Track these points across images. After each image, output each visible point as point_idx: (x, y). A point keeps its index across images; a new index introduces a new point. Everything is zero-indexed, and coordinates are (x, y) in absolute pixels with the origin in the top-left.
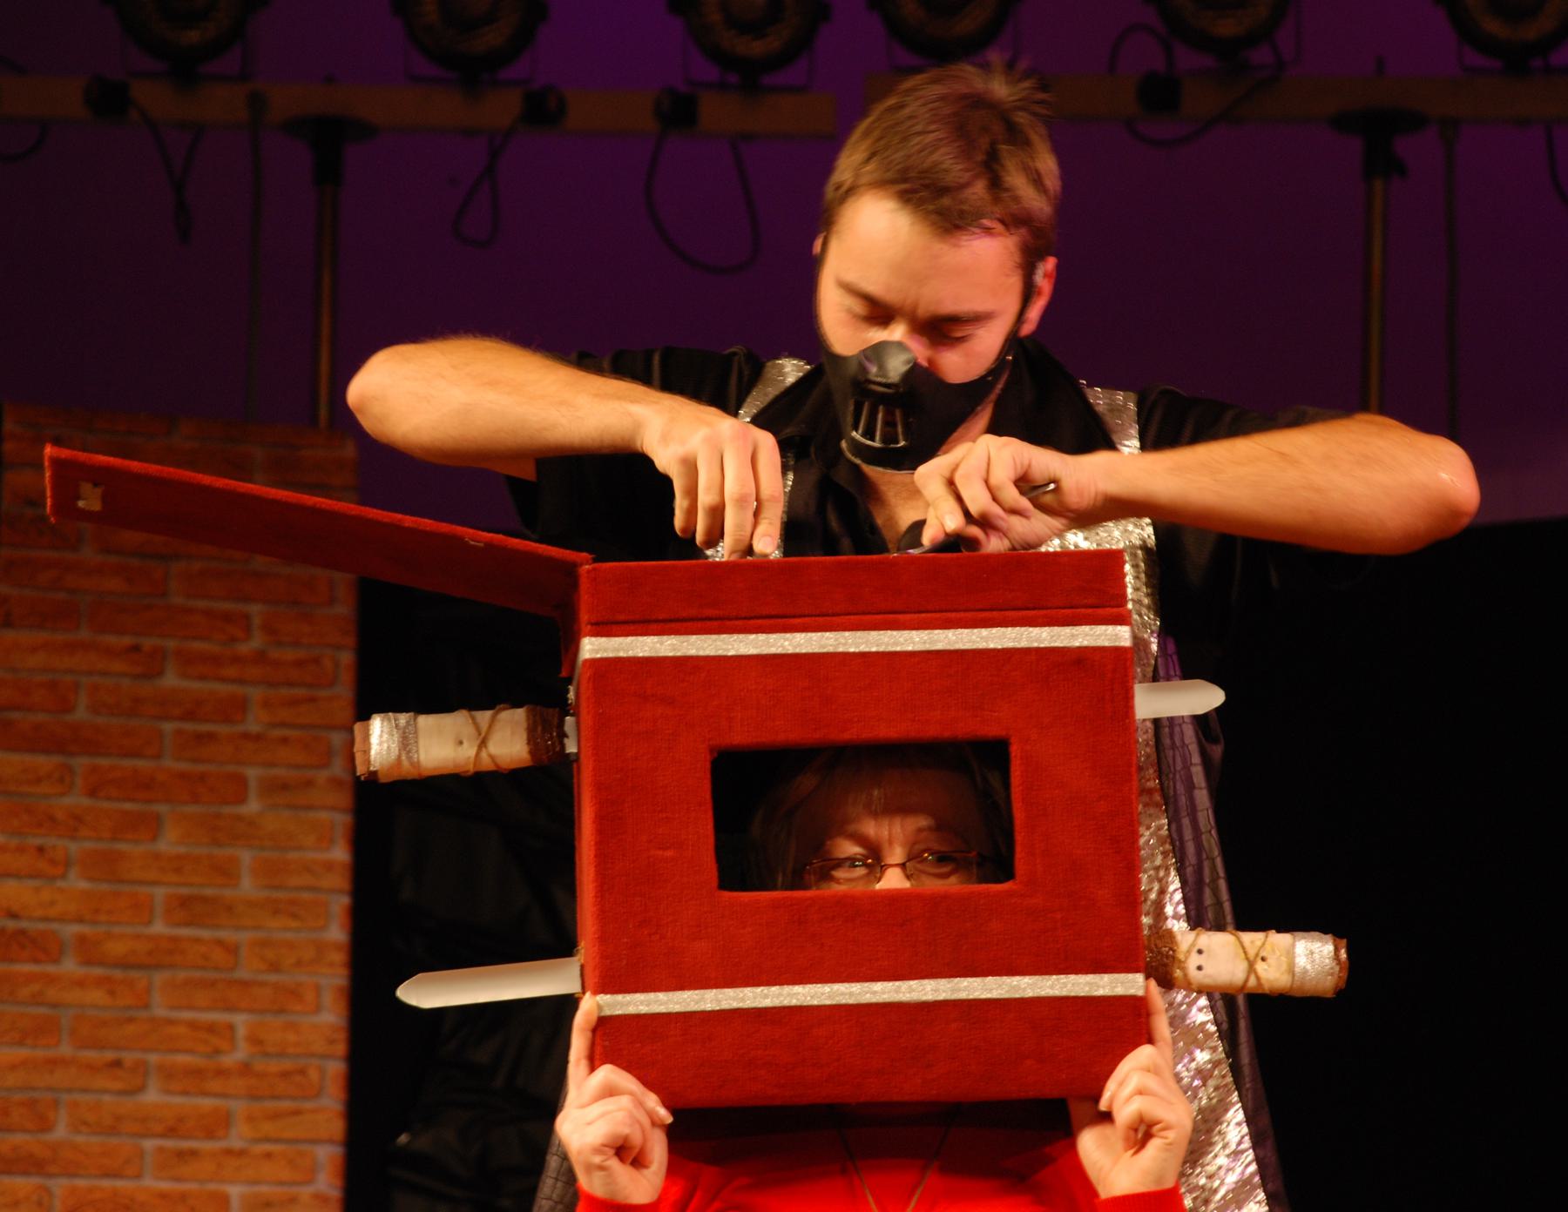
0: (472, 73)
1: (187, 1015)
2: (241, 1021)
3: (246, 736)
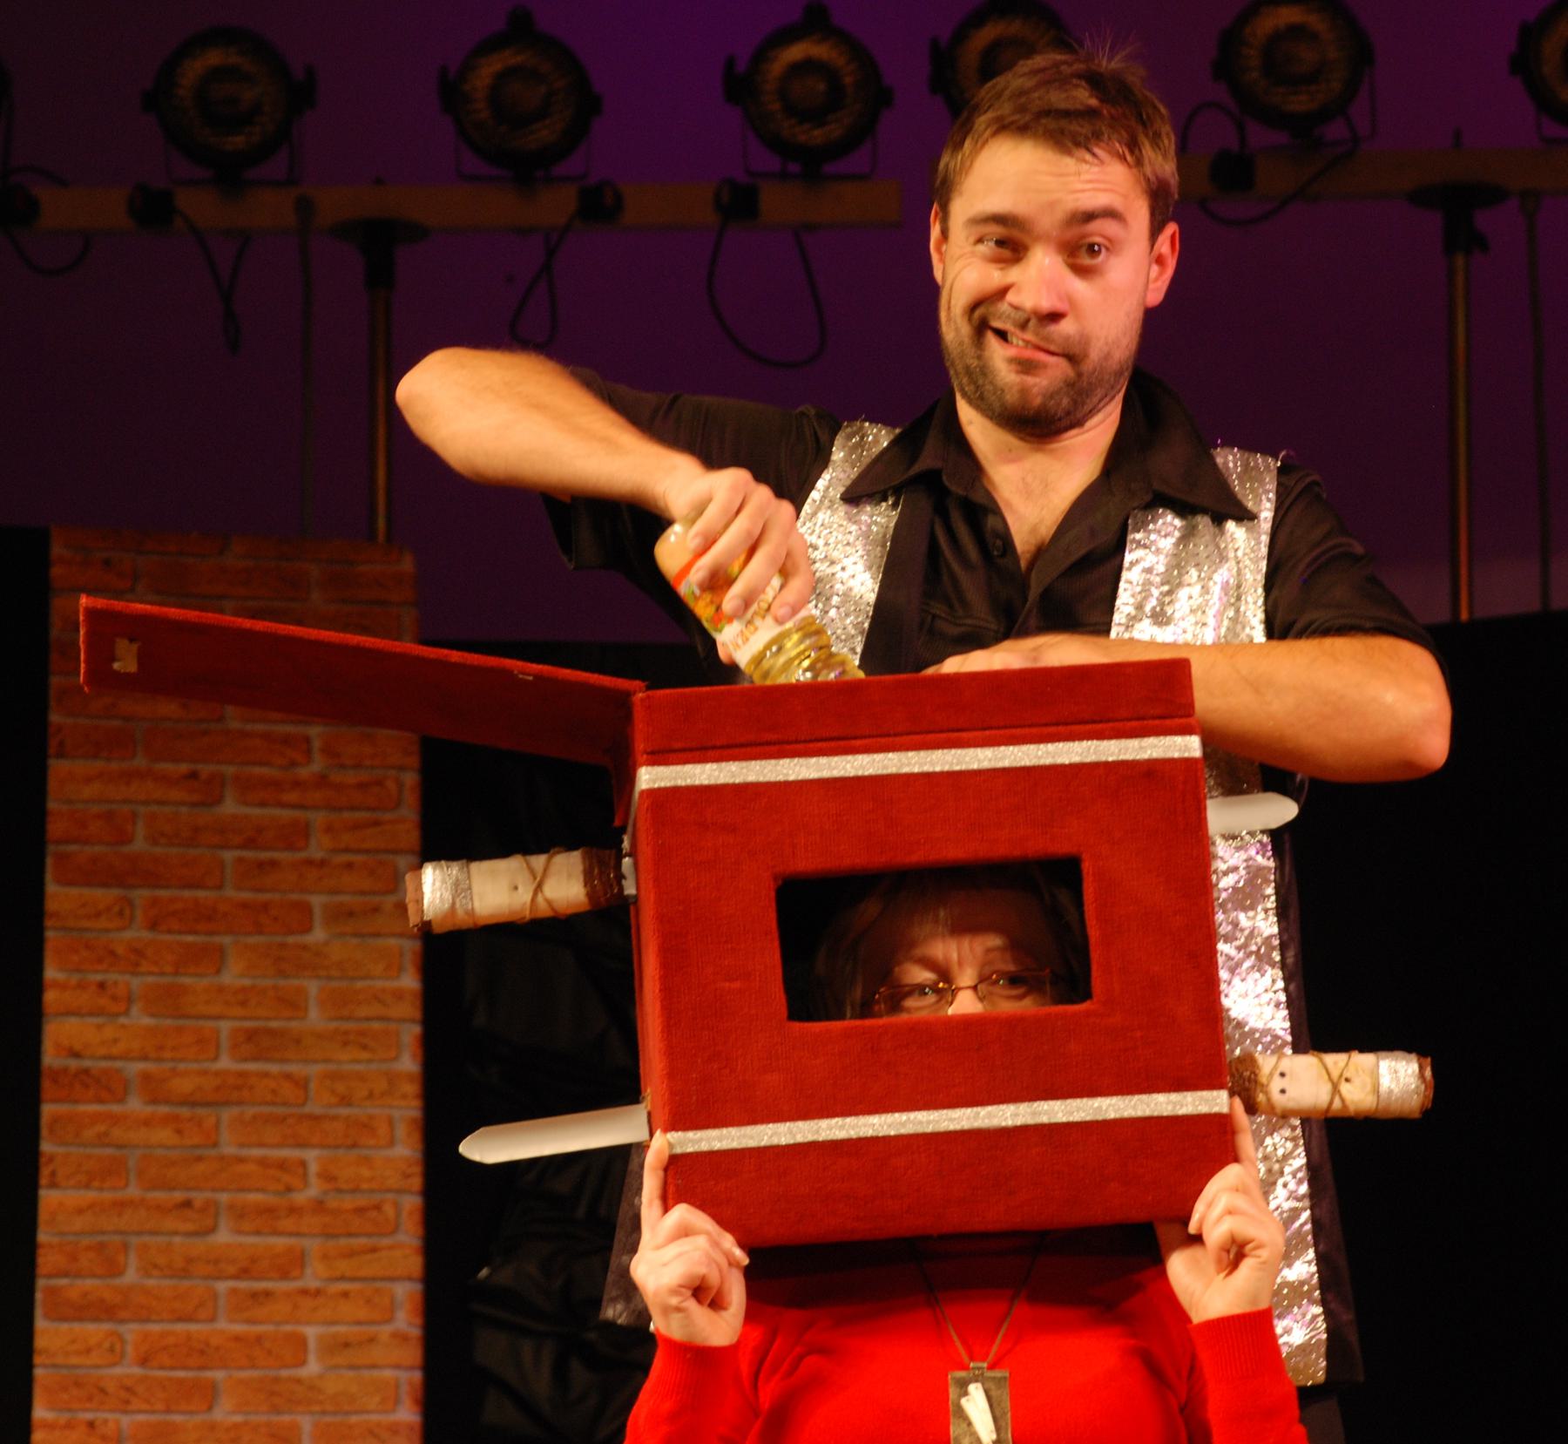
0: (526, 170)
1: (256, 1152)
2: (313, 1157)
3: (309, 862)
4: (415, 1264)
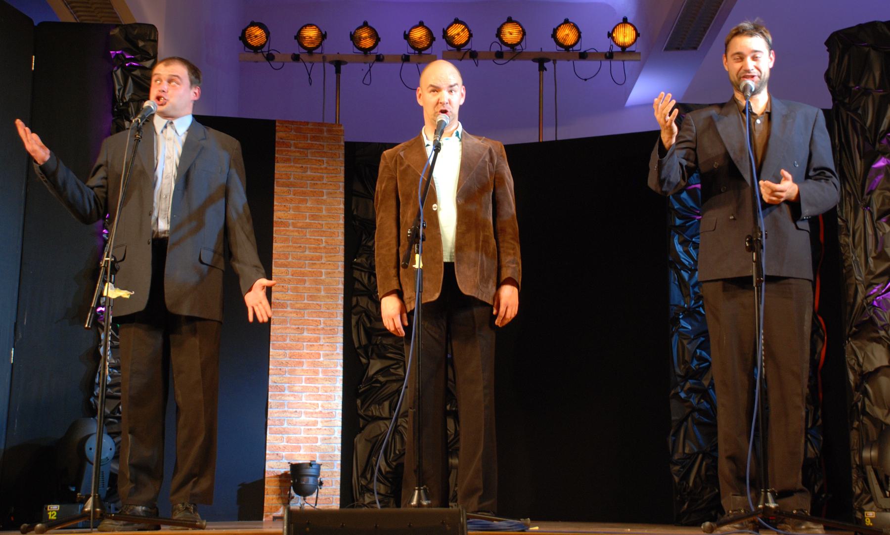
2: (324, 239)
4: (343, 259)
